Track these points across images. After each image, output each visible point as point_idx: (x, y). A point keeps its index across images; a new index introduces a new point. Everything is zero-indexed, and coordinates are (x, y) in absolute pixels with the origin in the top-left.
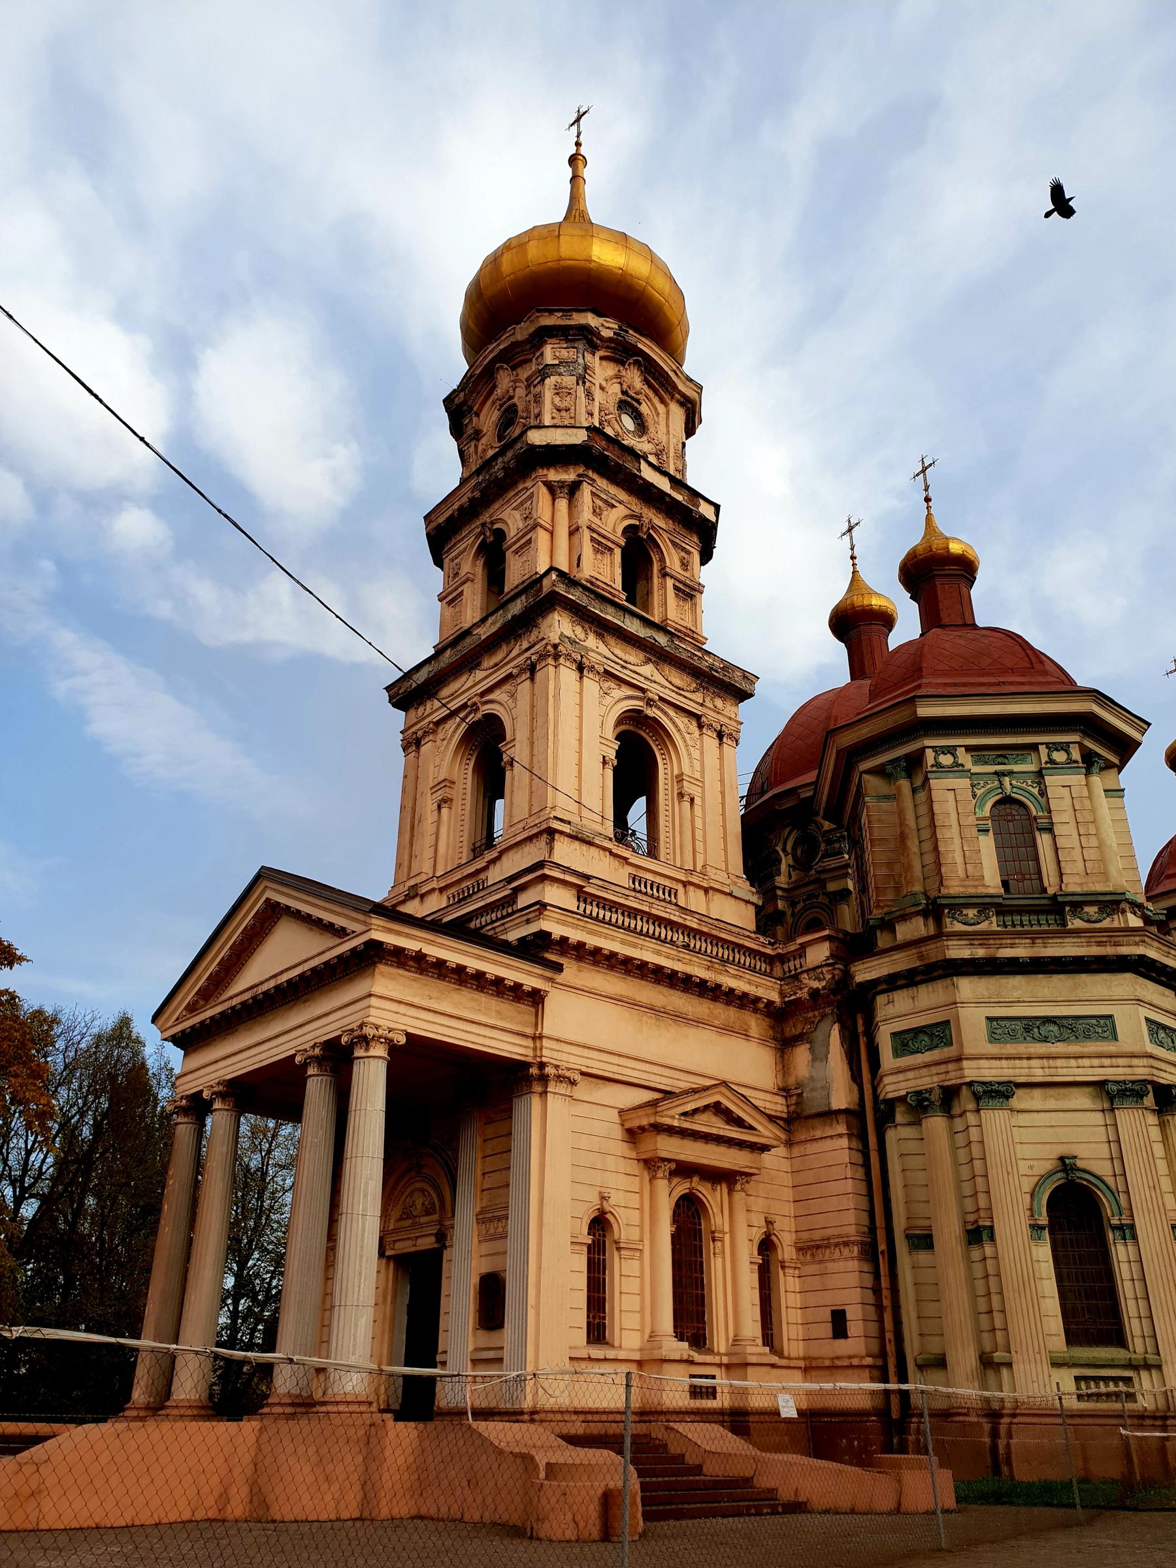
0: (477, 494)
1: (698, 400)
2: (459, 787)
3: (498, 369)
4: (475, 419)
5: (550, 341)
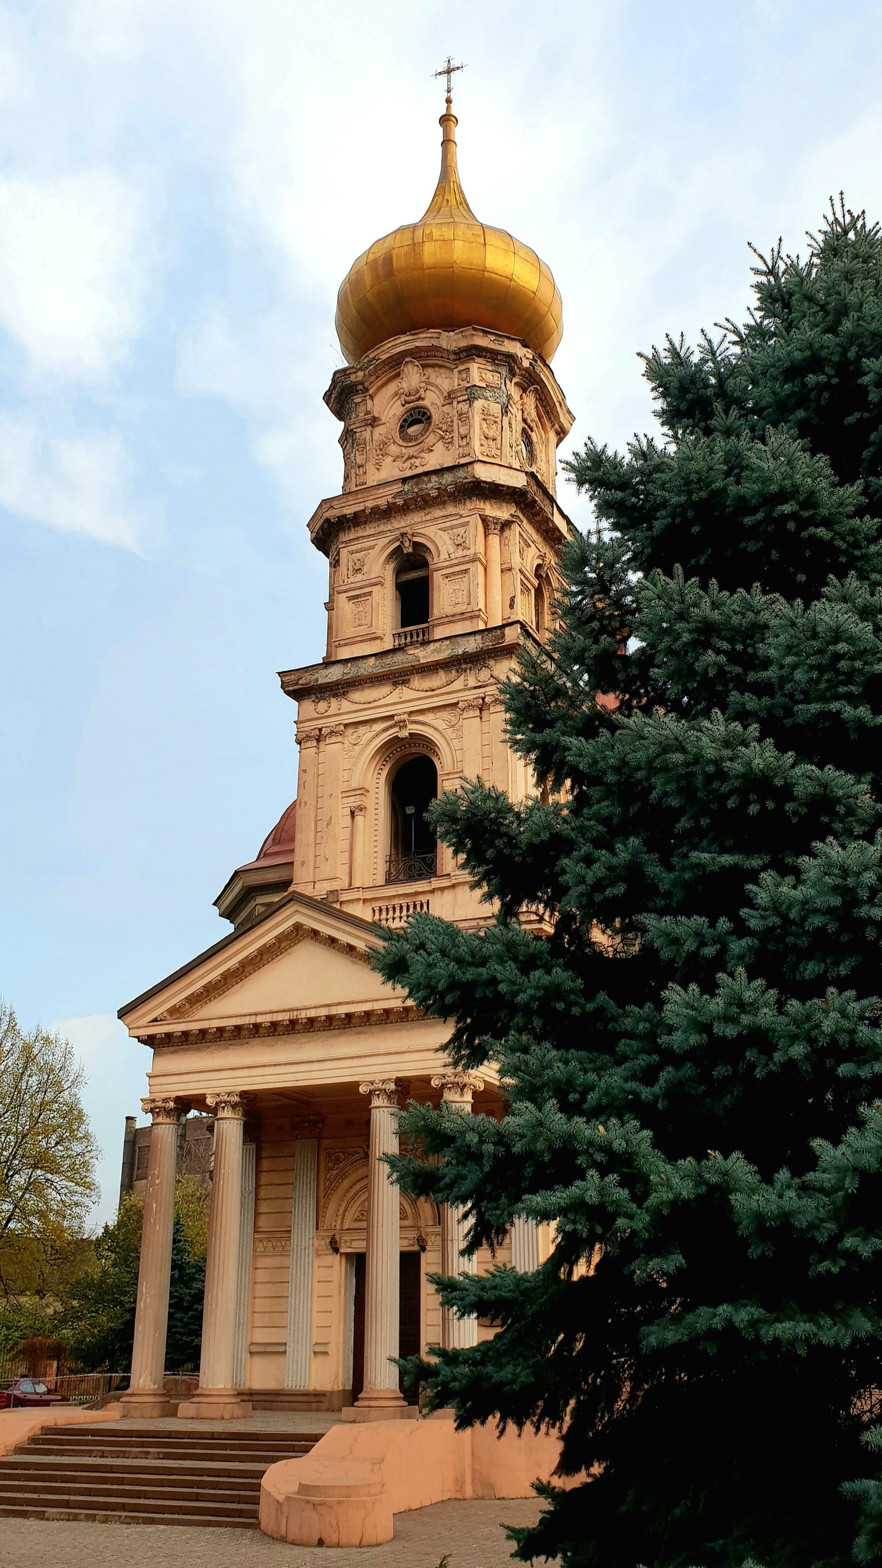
0: (400, 502)
2: (372, 795)
3: (407, 362)
4: (369, 402)
5: (478, 360)
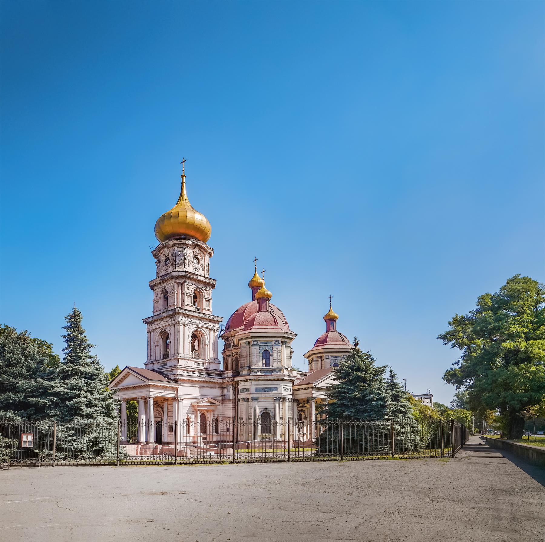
0: (161, 281)
1: (213, 252)
